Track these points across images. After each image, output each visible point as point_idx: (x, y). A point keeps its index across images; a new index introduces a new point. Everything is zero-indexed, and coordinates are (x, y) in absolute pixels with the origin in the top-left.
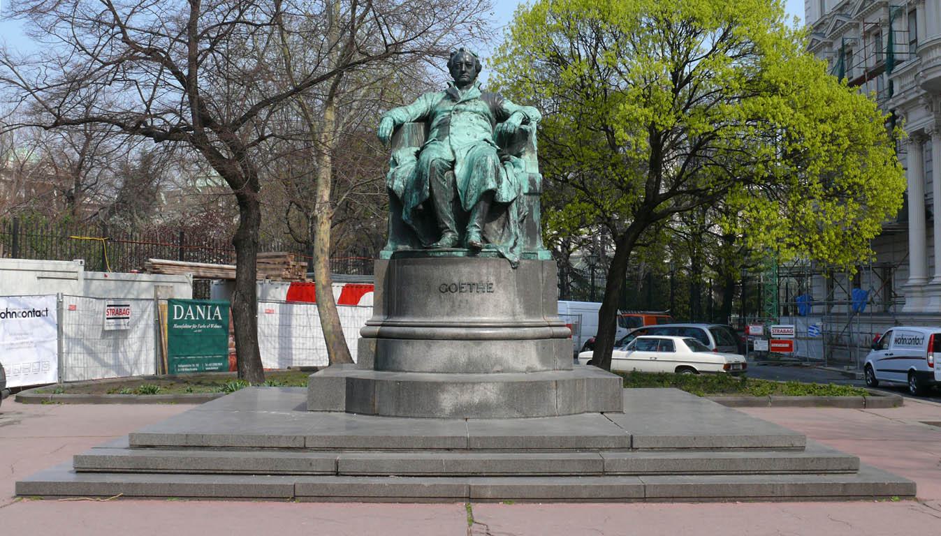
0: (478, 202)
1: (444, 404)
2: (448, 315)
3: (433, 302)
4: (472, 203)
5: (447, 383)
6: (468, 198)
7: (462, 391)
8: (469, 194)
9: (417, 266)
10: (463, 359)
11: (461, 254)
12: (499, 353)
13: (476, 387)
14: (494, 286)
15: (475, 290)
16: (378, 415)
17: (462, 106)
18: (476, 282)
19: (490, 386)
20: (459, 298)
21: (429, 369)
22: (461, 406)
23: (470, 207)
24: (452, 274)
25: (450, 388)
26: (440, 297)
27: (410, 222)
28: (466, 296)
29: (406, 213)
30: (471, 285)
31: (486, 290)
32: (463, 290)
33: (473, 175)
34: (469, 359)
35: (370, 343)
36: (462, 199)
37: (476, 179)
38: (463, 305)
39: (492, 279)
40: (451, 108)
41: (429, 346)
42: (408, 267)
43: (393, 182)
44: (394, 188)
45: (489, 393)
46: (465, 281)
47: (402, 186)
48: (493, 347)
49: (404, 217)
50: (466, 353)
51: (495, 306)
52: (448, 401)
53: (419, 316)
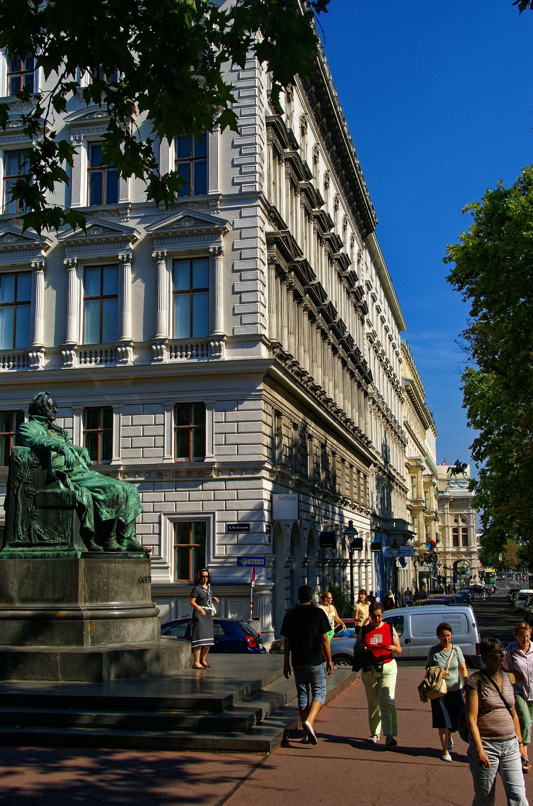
23: (129, 522)
27: (93, 530)
29: (91, 523)
37: (131, 502)
41: (144, 622)
42: (117, 565)
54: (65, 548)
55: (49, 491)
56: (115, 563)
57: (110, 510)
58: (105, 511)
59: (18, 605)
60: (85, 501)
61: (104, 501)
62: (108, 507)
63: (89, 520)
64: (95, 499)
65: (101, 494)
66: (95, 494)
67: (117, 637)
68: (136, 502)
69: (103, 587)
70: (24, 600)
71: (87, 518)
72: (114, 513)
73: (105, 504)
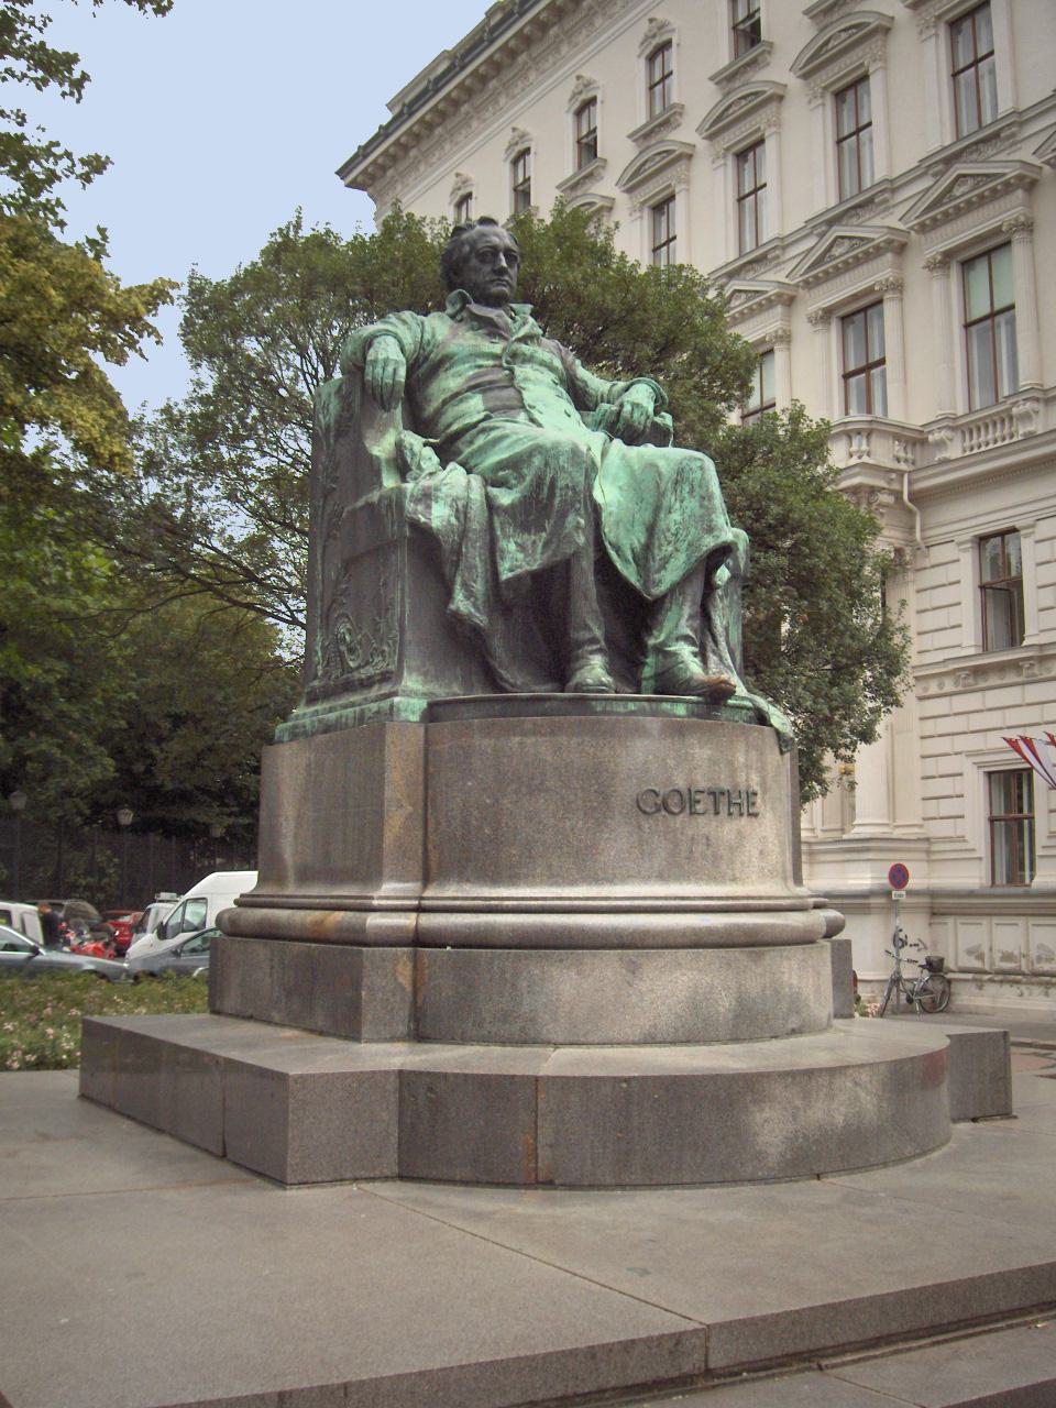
0: (686, 579)
1: (760, 1139)
2: (662, 877)
3: (617, 841)
4: (669, 577)
5: (767, 1075)
6: (654, 565)
7: (806, 1096)
8: (658, 554)
9: (563, 739)
10: (725, 1004)
11: (681, 710)
12: (795, 981)
13: (839, 1082)
14: (759, 800)
15: (723, 809)
16: (549, 1184)
17: (525, 348)
18: (725, 786)
19: (864, 1077)
20: (690, 833)
21: (637, 1034)
22: (806, 1138)
23: (663, 588)
24: (671, 762)
25: (777, 1089)
26: (640, 827)
27: (481, 619)
28: (705, 825)
29: (469, 594)
30: (715, 795)
31: (745, 810)
32: (699, 807)
33: (665, 503)
34: (740, 1000)
35: (396, 959)
36: (630, 573)
37: (676, 516)
38: (699, 848)
39: (755, 782)
40: (497, 348)
41: (634, 968)
42: (530, 741)
43: (429, 507)
44: (434, 525)
45: (863, 1095)
46: (703, 784)
47: (453, 520)
48: (785, 963)
49: (461, 603)
50: (734, 985)
51: (761, 853)
52: (771, 1127)
53: (573, 883)
54: (386, 689)
55: (360, 503)
56: (524, 734)
57: (528, 539)
58: (512, 547)
59: (291, 889)
60: (439, 516)
61: (510, 511)
62: (525, 528)
63: (465, 585)
64: (490, 504)
65: (510, 488)
66: (494, 491)
67: (505, 1017)
68: (699, 512)
69: (480, 828)
70: (305, 876)
71: (459, 580)
72: (539, 550)
73: (514, 519)
